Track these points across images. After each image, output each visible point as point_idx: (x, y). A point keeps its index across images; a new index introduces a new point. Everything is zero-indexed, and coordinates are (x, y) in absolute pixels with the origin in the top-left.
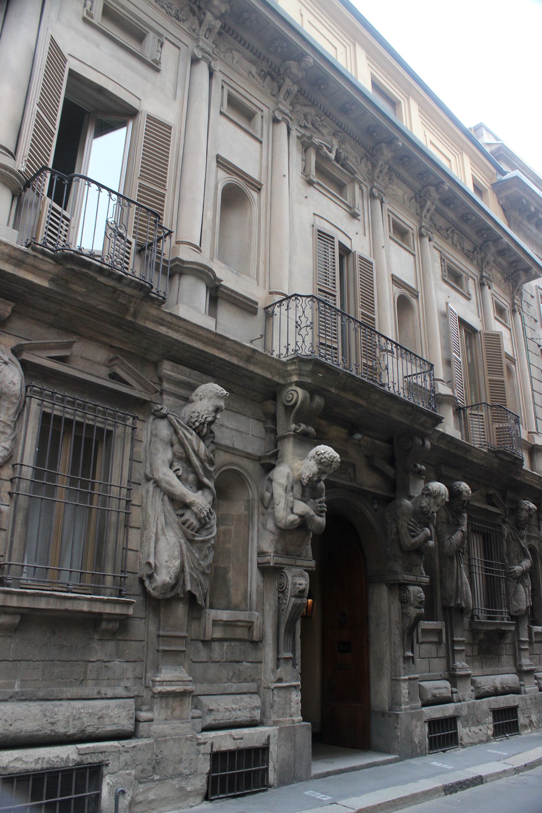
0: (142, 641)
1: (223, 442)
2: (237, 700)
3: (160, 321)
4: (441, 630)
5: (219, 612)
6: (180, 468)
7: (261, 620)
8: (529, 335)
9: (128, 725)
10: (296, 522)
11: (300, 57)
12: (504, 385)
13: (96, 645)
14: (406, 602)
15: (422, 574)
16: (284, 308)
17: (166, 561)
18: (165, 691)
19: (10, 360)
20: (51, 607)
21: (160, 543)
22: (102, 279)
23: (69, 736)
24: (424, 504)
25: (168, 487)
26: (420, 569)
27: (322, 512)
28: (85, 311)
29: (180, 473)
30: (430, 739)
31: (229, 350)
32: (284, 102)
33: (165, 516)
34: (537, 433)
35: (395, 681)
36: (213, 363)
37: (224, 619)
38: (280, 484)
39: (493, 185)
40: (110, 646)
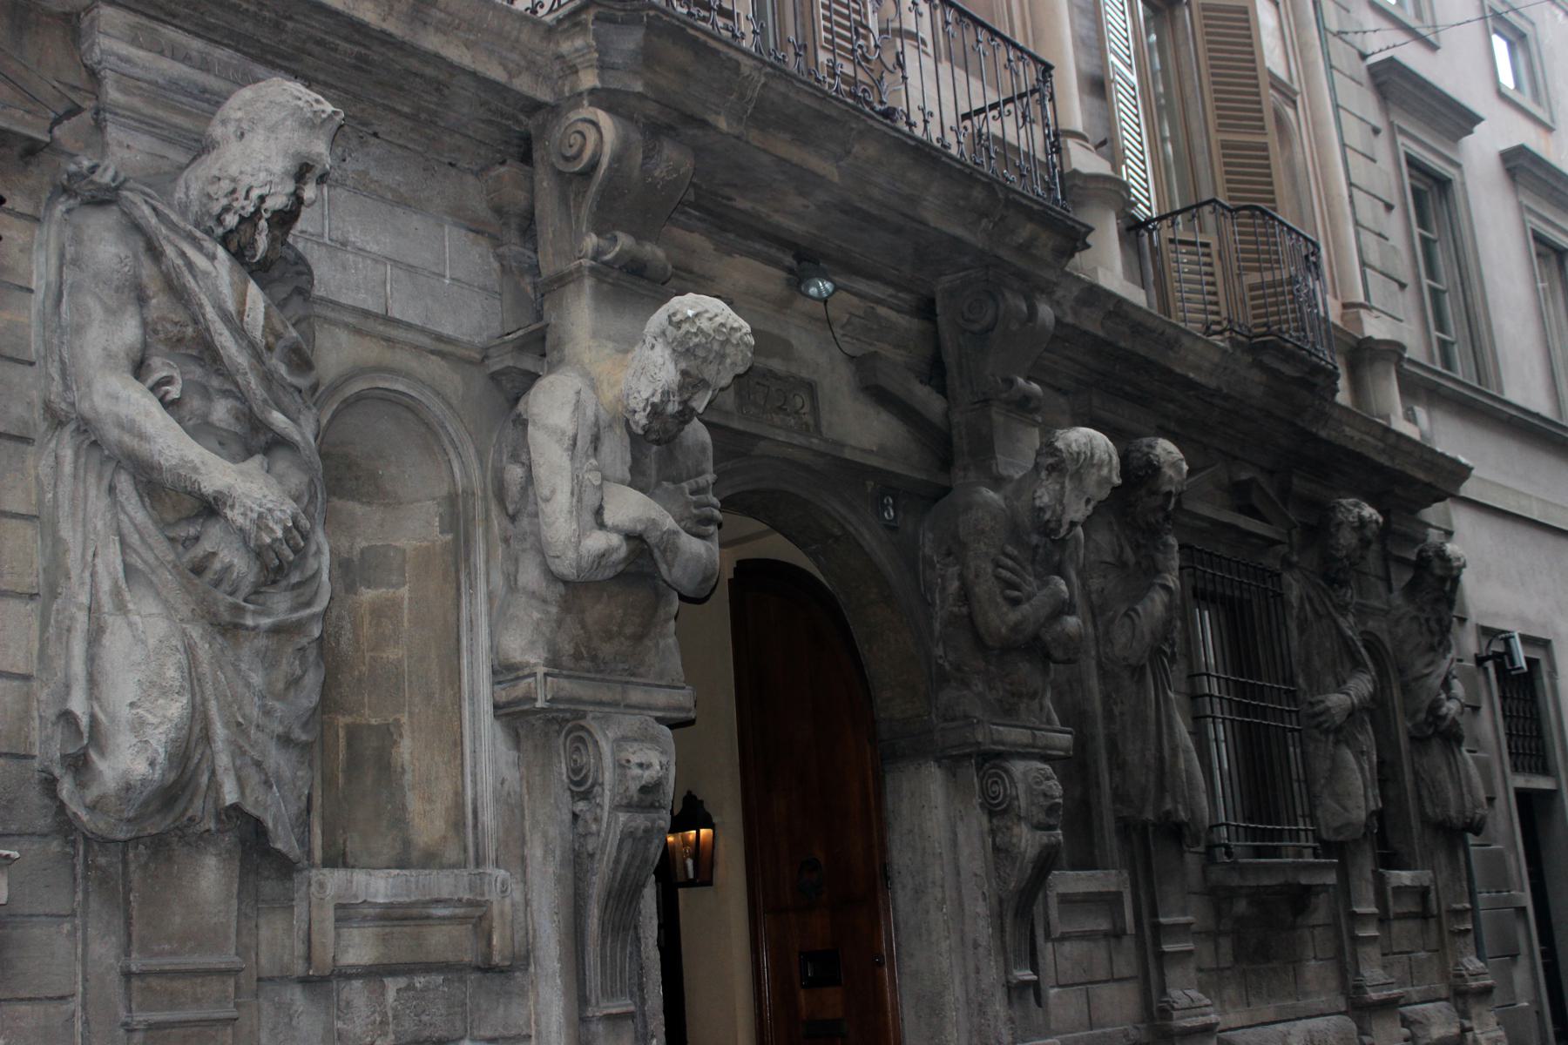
0: (62, 998)
4: (1119, 894)
5: (359, 877)
6: (176, 374)
7: (518, 896)
8: (1333, 26)
10: (615, 557)
12: (1267, 158)
14: (1005, 811)
15: (1049, 721)
17: (132, 705)
21: (107, 640)
24: (1044, 497)
26: (1042, 708)
27: (709, 520)
29: (174, 392)
33: (124, 544)
34: (1369, 308)
36: (290, 25)
38: (553, 431)
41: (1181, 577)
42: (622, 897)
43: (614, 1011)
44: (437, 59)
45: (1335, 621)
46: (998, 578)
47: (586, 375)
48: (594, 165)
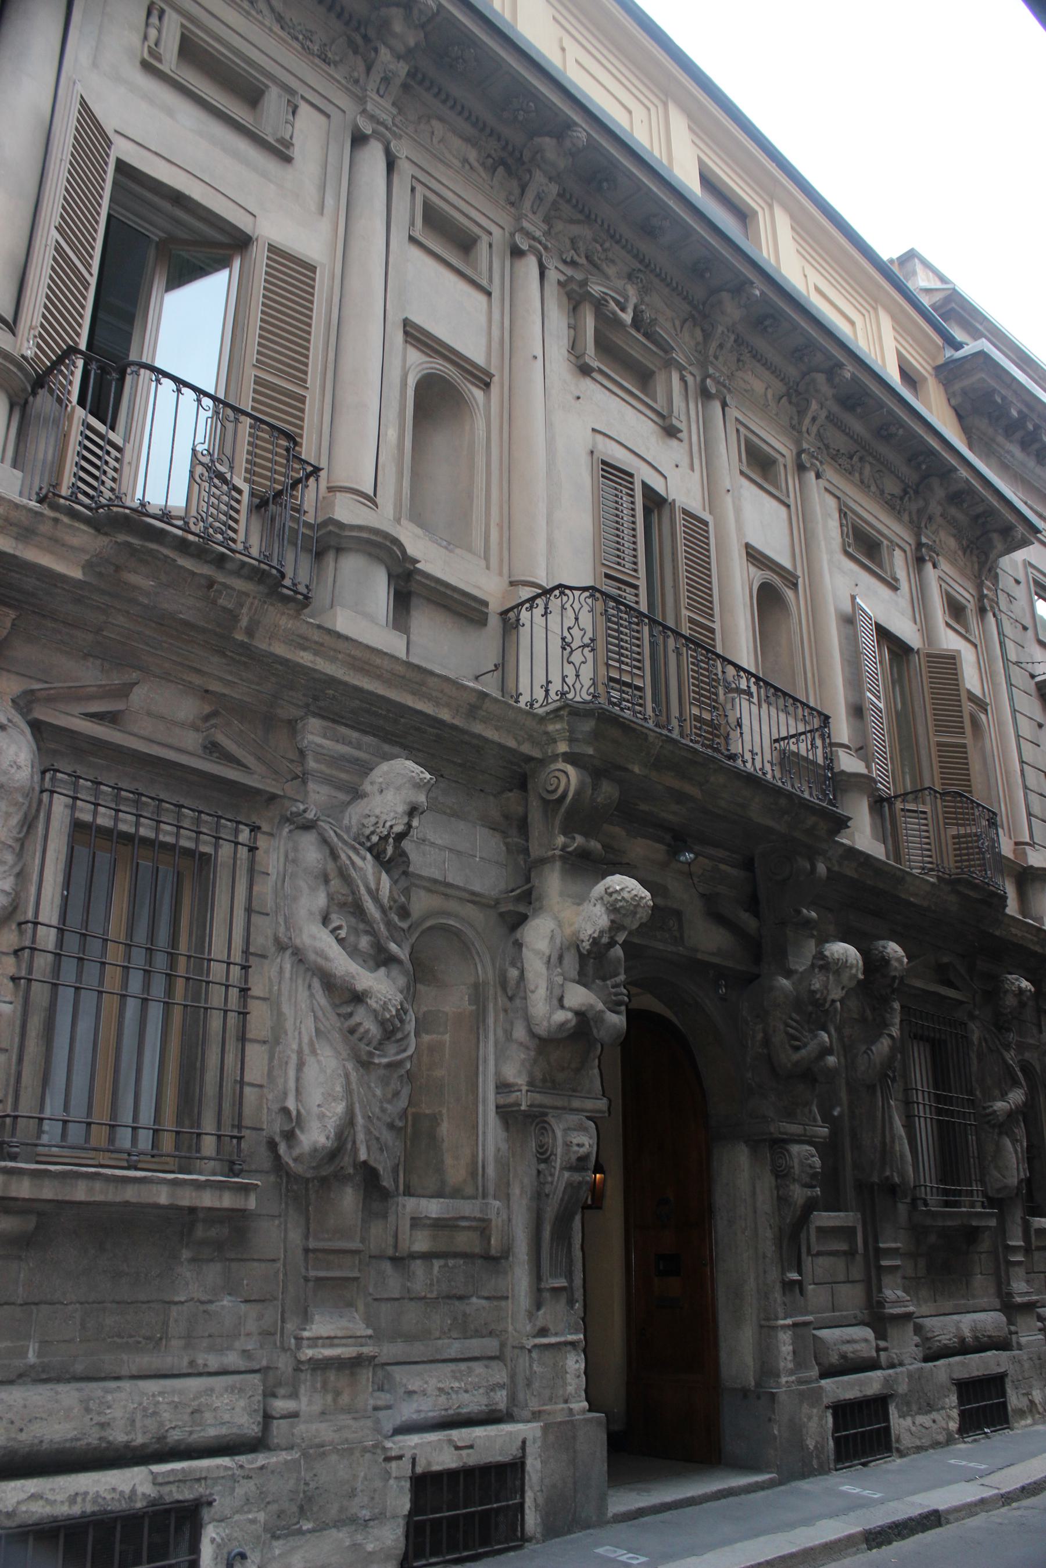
0: (273, 1260)
1: (425, 873)
2: (460, 1371)
5: (424, 1202)
6: (344, 924)
7: (505, 1217)
8: (1013, 656)
9: (247, 1424)
10: (569, 1025)
11: (562, 129)
13: (186, 1272)
15: (815, 1120)
16: (538, 611)
17: (319, 1106)
18: (320, 1356)
19: (10, 721)
20: (99, 1198)
21: (306, 1069)
23: (135, 1449)
24: (816, 985)
25: (320, 961)
26: (810, 1111)
27: (619, 1003)
28: (154, 625)
29: (343, 933)
30: (837, 1441)
31: (434, 694)
32: (530, 215)
33: (315, 1017)
34: (1032, 844)
35: (767, 1329)
36: (403, 720)
37: (434, 1216)
38: (537, 952)
39: (938, 369)
40: (213, 1272)
41: (901, 1029)
42: (563, 1222)
43: (556, 1285)
44: (479, 737)
45: (1002, 1054)
46: (787, 1033)
47: (556, 918)
48: (564, 796)
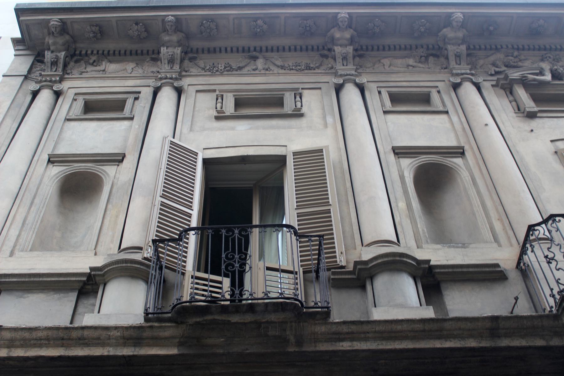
3: (334, 336)
11: (447, 21)
22: (235, 319)
32: (457, 66)
